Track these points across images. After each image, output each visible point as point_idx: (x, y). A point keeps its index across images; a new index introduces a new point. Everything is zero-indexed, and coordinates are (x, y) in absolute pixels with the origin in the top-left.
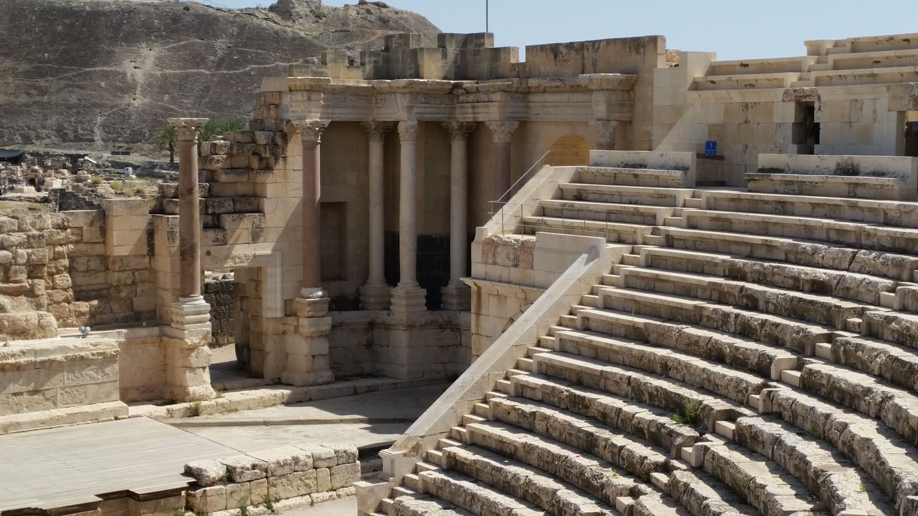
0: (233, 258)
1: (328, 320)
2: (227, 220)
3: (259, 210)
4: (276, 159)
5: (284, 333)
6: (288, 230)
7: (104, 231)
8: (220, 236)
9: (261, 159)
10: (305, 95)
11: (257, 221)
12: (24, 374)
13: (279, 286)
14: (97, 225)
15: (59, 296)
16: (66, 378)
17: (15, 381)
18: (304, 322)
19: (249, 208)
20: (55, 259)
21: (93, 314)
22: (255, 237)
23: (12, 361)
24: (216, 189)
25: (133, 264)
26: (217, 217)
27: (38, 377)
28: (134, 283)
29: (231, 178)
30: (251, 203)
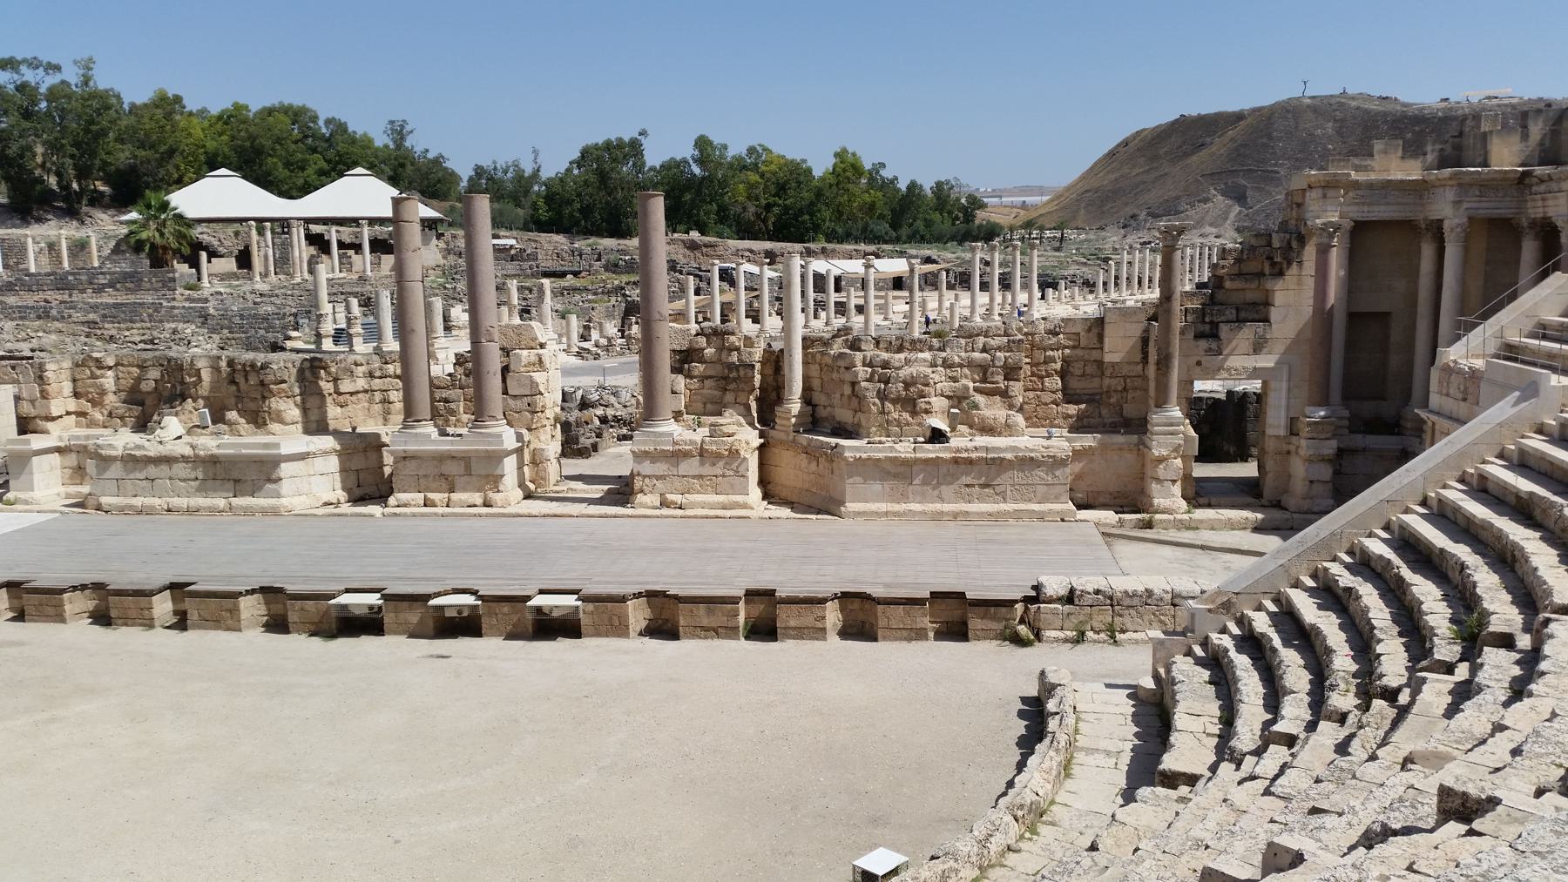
0: (1228, 370)
1: (1334, 444)
2: (1224, 330)
3: (1266, 320)
4: (1289, 264)
5: (1289, 453)
6: (1296, 342)
7: (1101, 337)
8: (1214, 346)
9: (1273, 264)
10: (1320, 191)
11: (1260, 331)
12: (976, 468)
13: (1283, 402)
14: (1095, 331)
15: (1047, 397)
16: (1017, 476)
17: (967, 474)
18: (1303, 443)
19: (1256, 316)
20: (1045, 362)
21: (1080, 417)
22: (1257, 348)
23: (965, 455)
24: (1220, 296)
25: (1125, 370)
26: (1215, 325)
27: (988, 473)
28: (1125, 389)
29: (1237, 284)
30: (1258, 311)
